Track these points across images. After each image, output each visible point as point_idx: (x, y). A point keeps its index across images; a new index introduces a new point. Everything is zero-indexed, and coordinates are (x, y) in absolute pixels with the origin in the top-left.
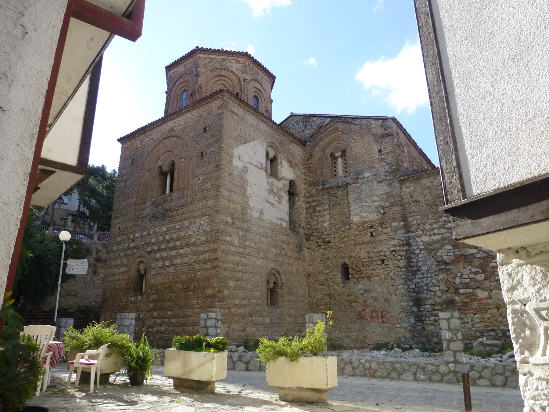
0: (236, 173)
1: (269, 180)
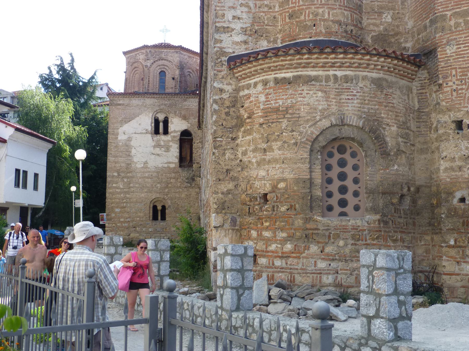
0: (121, 144)
1: (155, 139)
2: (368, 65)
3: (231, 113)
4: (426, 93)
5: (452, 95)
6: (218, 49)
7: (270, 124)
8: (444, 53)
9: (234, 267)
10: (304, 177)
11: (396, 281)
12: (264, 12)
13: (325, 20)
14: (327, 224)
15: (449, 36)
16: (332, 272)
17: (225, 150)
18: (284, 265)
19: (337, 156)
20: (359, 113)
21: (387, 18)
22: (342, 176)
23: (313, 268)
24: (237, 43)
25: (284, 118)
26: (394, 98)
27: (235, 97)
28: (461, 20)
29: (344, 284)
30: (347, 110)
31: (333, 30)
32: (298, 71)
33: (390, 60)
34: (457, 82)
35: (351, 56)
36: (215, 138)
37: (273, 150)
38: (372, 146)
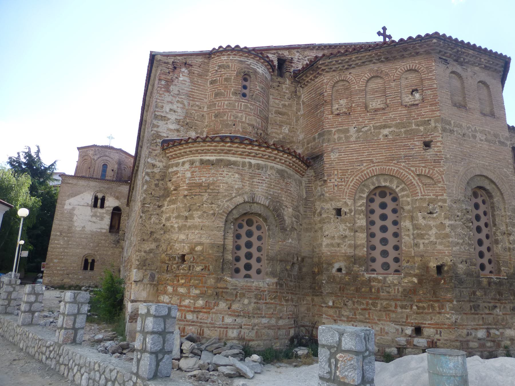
2: (276, 158)
3: (160, 185)
4: (312, 186)
5: (334, 189)
6: (155, 132)
7: (193, 196)
8: (329, 157)
9: (155, 330)
10: (219, 243)
11: (363, 367)
12: (195, 110)
13: (242, 122)
14: (235, 285)
15: (333, 146)
16: (236, 327)
17: (151, 215)
18: (195, 319)
19: (246, 228)
20: (266, 195)
21: (286, 130)
22: (249, 245)
23: (221, 322)
24: (171, 130)
25: (206, 192)
26: (291, 187)
27: (164, 172)
28: (342, 136)
29: (246, 338)
30: (257, 191)
31: (248, 130)
32: (221, 156)
33: (291, 157)
34: (338, 180)
35: (263, 149)
36: (144, 204)
37: (194, 218)
38: (274, 222)
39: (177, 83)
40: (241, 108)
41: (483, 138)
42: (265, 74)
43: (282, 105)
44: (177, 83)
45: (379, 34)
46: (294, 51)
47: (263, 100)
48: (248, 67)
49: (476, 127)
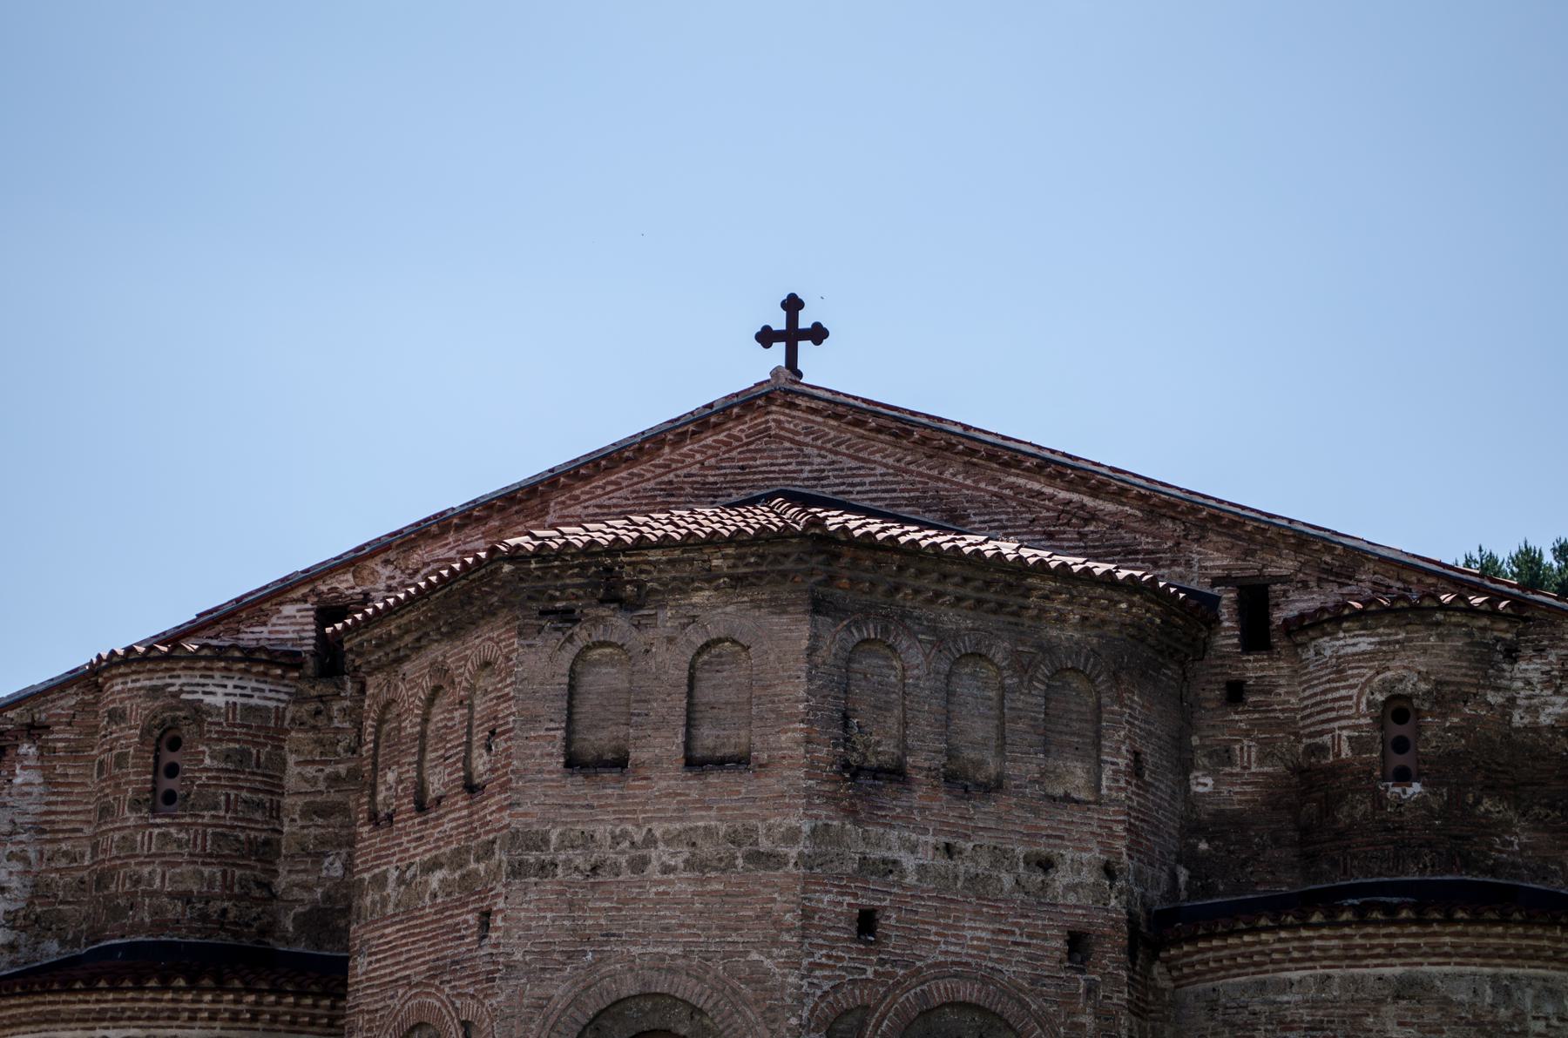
21: (334, 868)
31: (170, 916)
39: (8, 799)
40: (149, 849)
41: (678, 861)
42: (239, 700)
43: (328, 778)
44: (8, 799)
45: (766, 337)
46: (375, 564)
47: (233, 793)
48: (174, 701)
49: (654, 825)
